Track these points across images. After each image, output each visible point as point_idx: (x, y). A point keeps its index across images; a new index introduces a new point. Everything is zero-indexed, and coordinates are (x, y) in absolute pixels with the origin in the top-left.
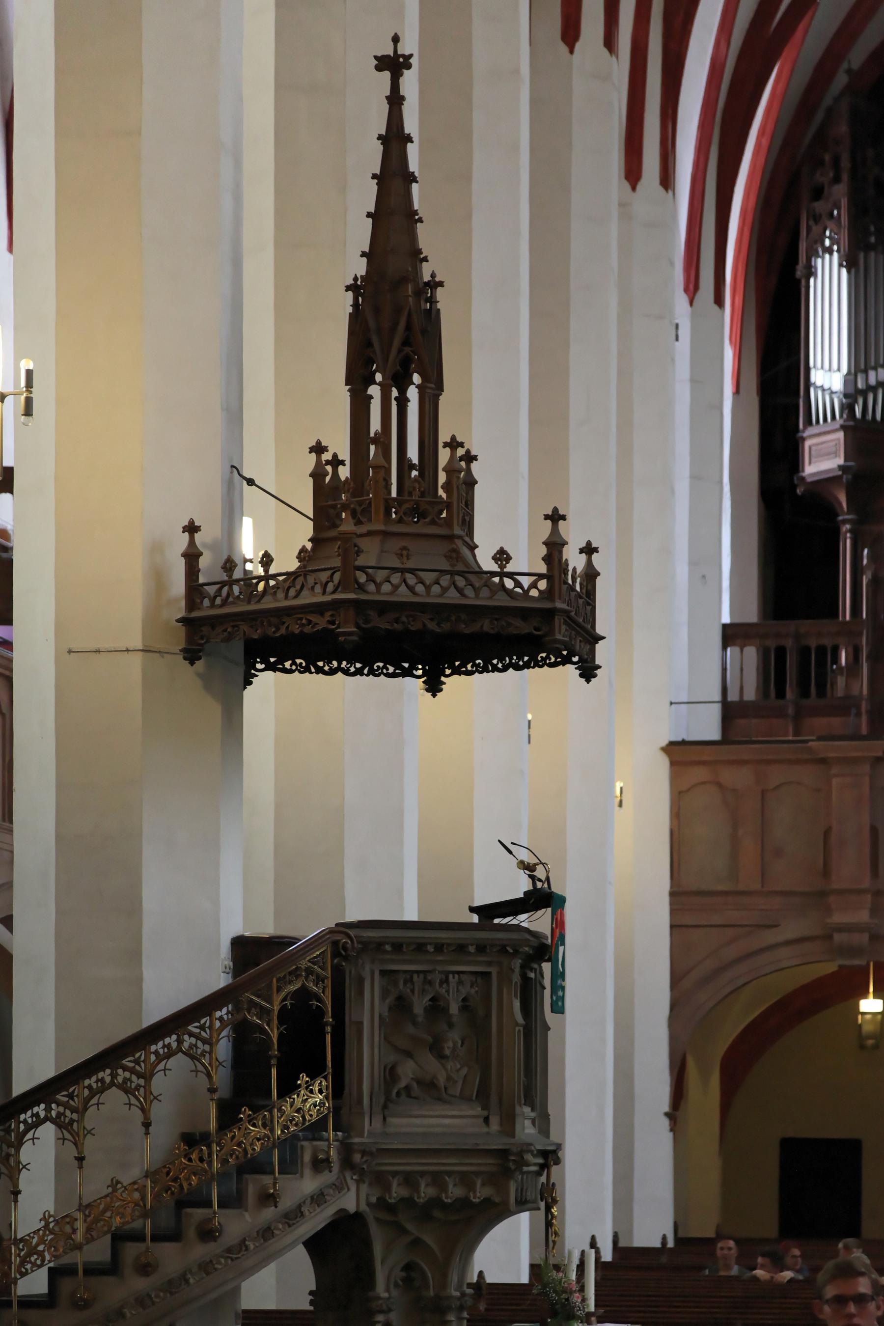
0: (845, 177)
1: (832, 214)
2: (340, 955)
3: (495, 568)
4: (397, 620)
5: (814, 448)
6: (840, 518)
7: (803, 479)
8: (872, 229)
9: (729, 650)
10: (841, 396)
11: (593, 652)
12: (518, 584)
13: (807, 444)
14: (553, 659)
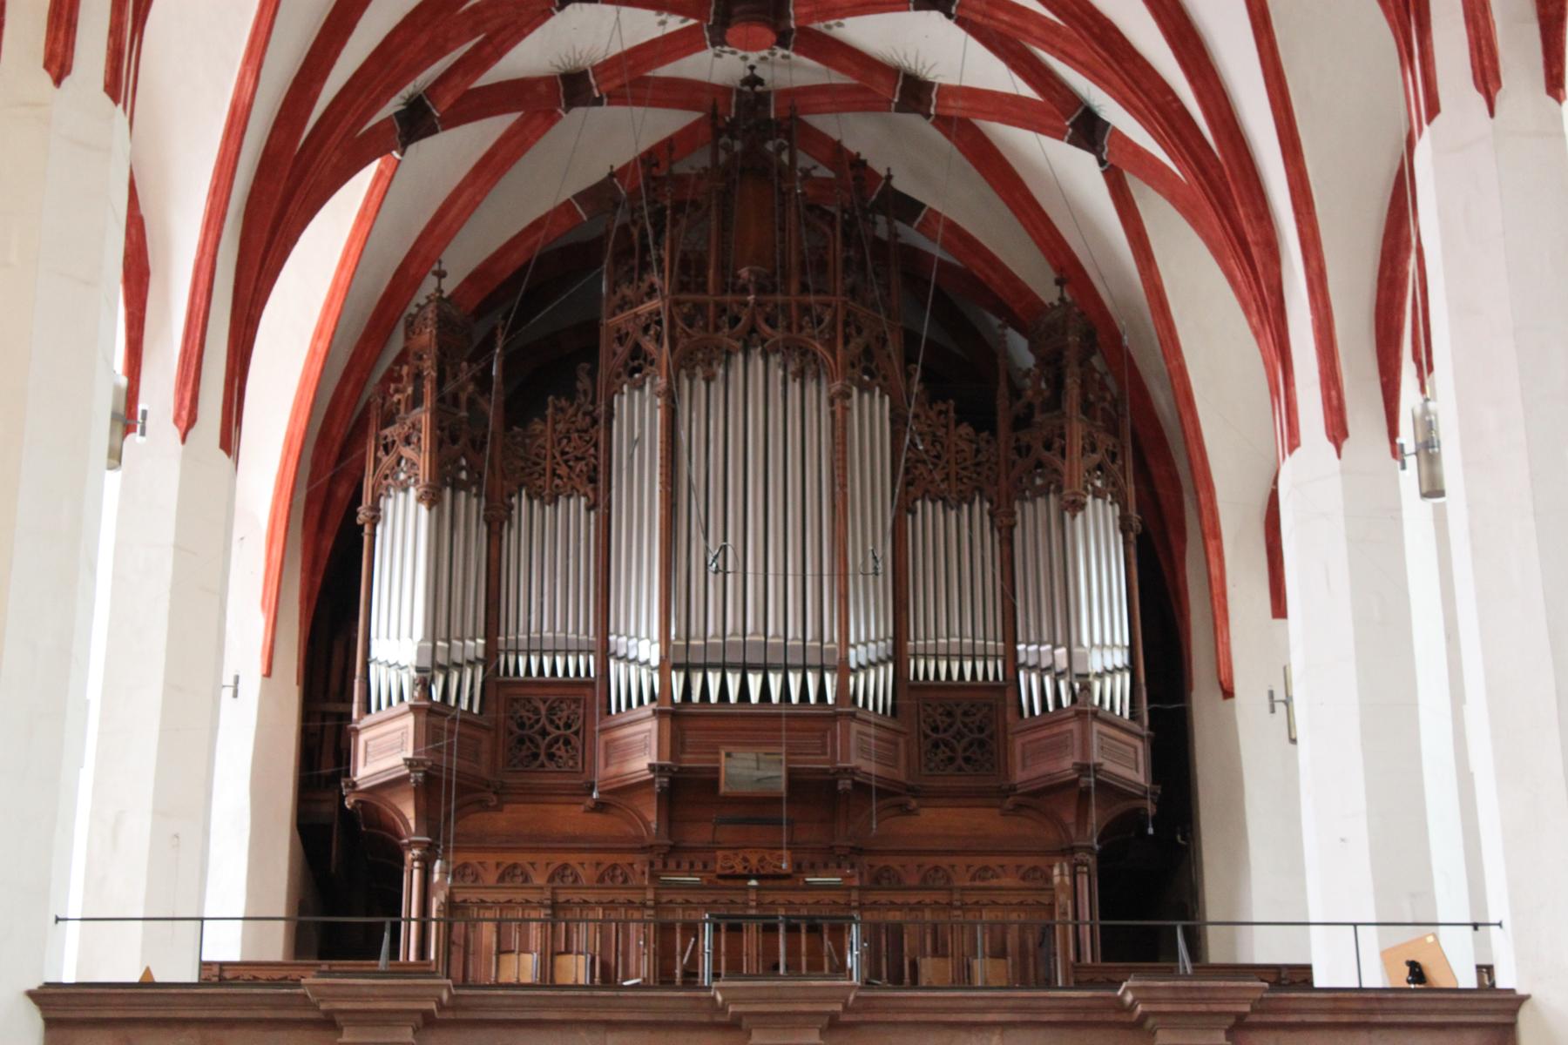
0: (428, 388)
6: (405, 841)
7: (355, 784)
10: (414, 674)
13: (362, 738)
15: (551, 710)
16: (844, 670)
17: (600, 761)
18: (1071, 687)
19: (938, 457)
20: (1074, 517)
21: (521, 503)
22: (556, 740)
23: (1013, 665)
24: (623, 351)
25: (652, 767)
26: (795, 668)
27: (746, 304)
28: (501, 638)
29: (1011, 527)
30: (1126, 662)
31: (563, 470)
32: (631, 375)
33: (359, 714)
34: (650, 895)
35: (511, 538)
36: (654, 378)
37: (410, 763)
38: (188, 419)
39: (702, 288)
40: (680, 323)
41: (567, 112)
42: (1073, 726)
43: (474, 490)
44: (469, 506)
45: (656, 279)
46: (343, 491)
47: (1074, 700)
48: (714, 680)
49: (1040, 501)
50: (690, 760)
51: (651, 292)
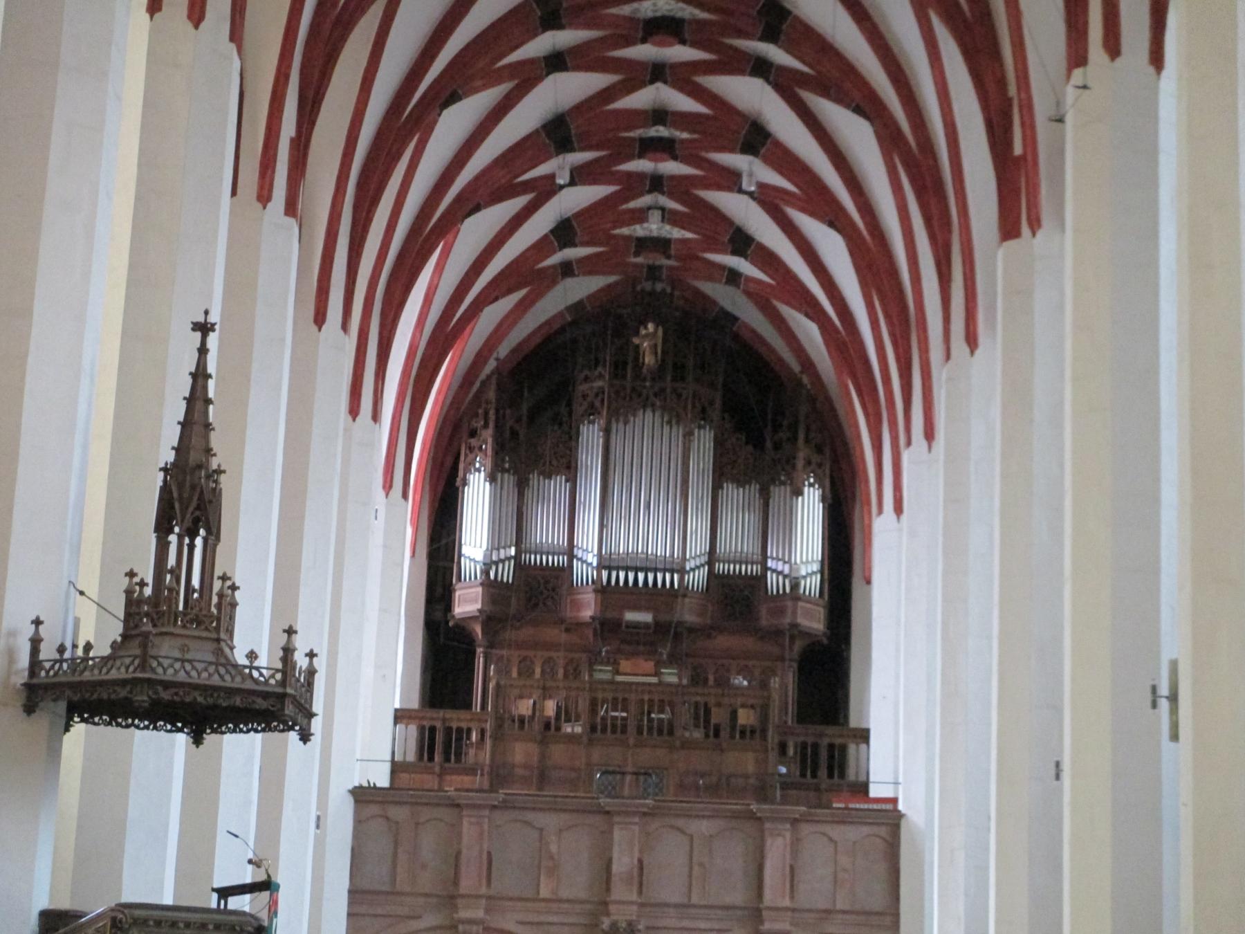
0: (491, 425)
1: (481, 446)
2: (117, 927)
3: (246, 662)
4: (176, 694)
5: (461, 598)
7: (453, 616)
8: (507, 459)
9: (398, 726)
10: (482, 564)
11: (309, 724)
12: (261, 675)
13: (457, 594)
14: (281, 727)
15: (547, 582)
16: (682, 572)
17: (568, 610)
18: (790, 582)
19: (735, 462)
20: (797, 499)
21: (534, 479)
22: (548, 597)
23: (765, 568)
24: (585, 404)
25: (592, 618)
26: (660, 570)
27: (645, 387)
28: (523, 546)
29: (768, 499)
30: (819, 568)
31: (555, 463)
32: (590, 415)
33: (456, 581)
34: (587, 685)
35: (528, 494)
36: (599, 420)
37: (480, 611)
38: (388, 486)
39: (624, 377)
40: (613, 395)
41: (562, 280)
42: (789, 604)
43: (512, 472)
44: (509, 480)
45: (603, 372)
46: (449, 461)
47: (792, 589)
48: (622, 575)
49: (783, 487)
50: (610, 615)
51: (601, 376)
